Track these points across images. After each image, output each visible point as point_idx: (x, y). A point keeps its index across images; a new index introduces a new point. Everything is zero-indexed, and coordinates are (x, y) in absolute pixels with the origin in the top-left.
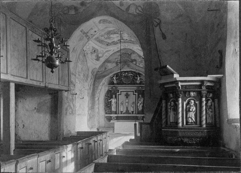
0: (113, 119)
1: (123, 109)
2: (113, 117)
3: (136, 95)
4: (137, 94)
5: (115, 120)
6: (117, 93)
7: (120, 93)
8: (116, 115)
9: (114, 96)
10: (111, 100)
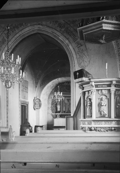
1: (65, 109)
8: (60, 114)
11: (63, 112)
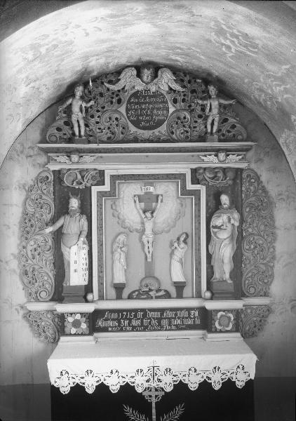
0: (73, 331)
2: (70, 319)
3: (196, 194)
4: (202, 189)
5: (82, 334)
7: (106, 188)
8: (89, 308)
9: (74, 203)
10: (58, 224)
11: (112, 293)
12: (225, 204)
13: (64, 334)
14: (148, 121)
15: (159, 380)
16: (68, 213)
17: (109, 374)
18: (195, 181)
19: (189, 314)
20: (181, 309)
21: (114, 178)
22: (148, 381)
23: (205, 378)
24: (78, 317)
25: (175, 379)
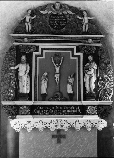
3: (79, 57)
4: (81, 54)
6: (34, 54)
12: (90, 60)
13: (19, 115)
14: (58, 26)
15: (62, 126)
16: (21, 63)
17: (38, 123)
18: (78, 51)
19: (75, 108)
20: (71, 106)
21: (43, 49)
22: (56, 126)
23: (83, 125)
24: (25, 107)
25: (69, 125)
